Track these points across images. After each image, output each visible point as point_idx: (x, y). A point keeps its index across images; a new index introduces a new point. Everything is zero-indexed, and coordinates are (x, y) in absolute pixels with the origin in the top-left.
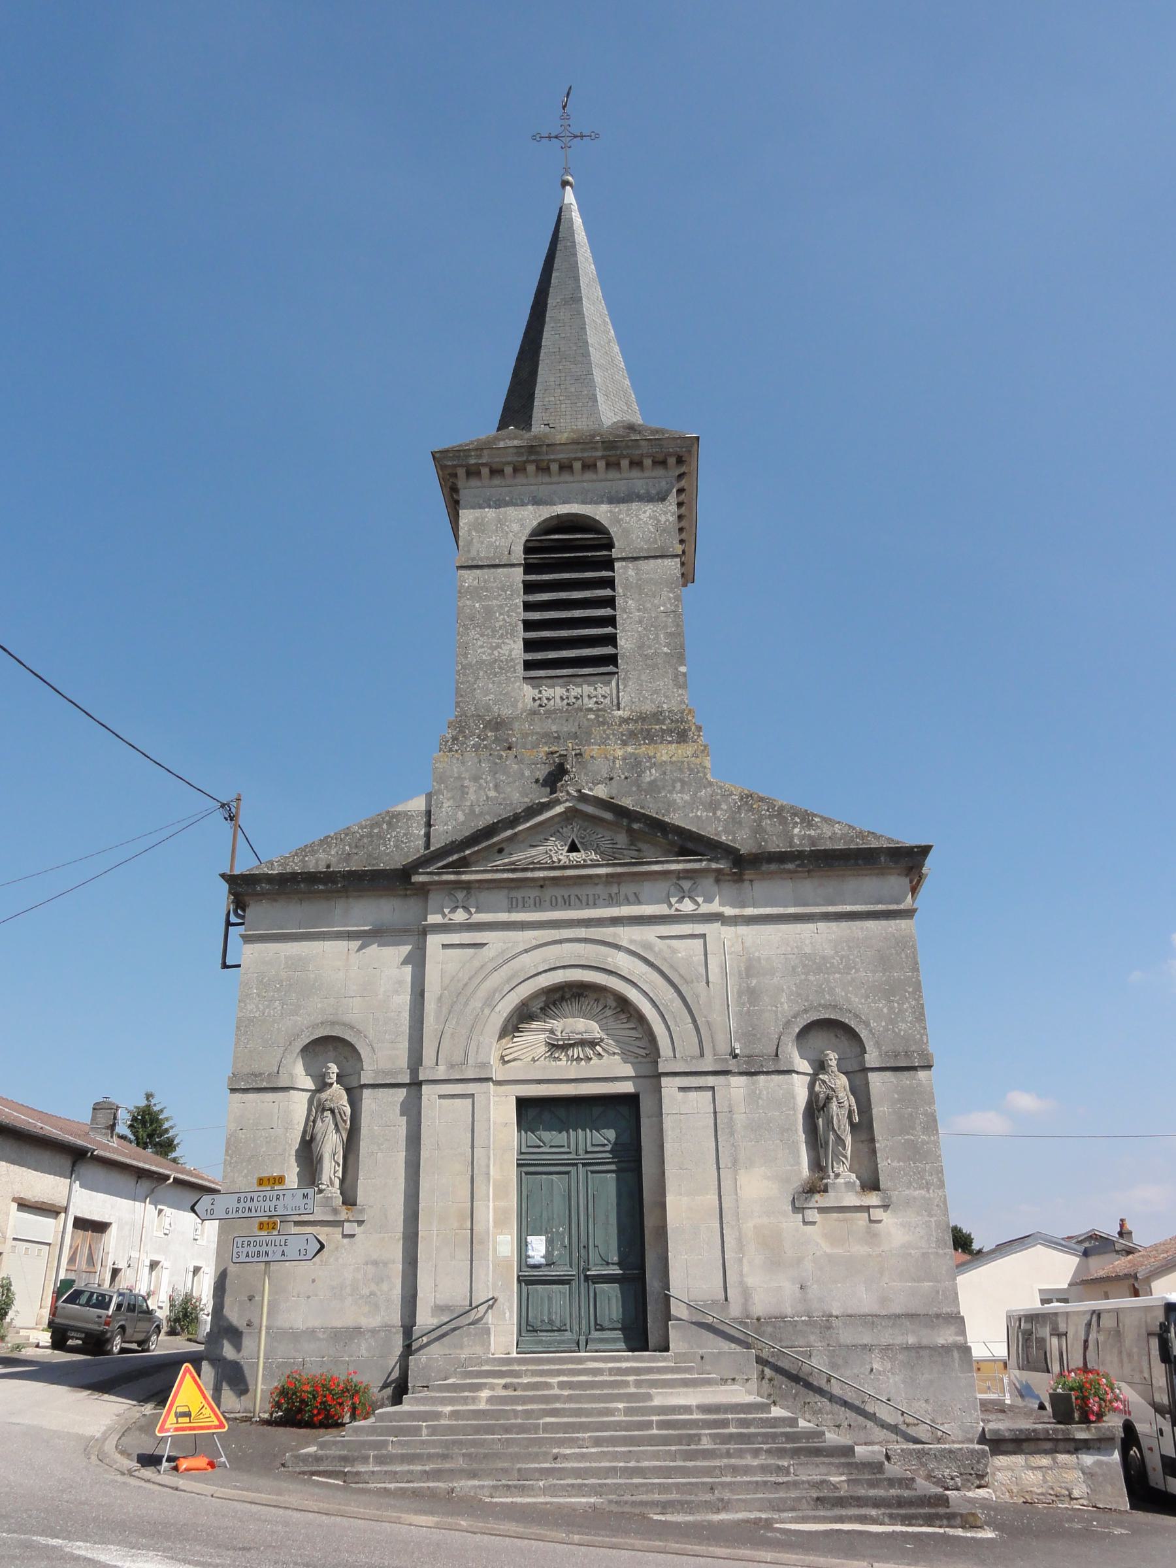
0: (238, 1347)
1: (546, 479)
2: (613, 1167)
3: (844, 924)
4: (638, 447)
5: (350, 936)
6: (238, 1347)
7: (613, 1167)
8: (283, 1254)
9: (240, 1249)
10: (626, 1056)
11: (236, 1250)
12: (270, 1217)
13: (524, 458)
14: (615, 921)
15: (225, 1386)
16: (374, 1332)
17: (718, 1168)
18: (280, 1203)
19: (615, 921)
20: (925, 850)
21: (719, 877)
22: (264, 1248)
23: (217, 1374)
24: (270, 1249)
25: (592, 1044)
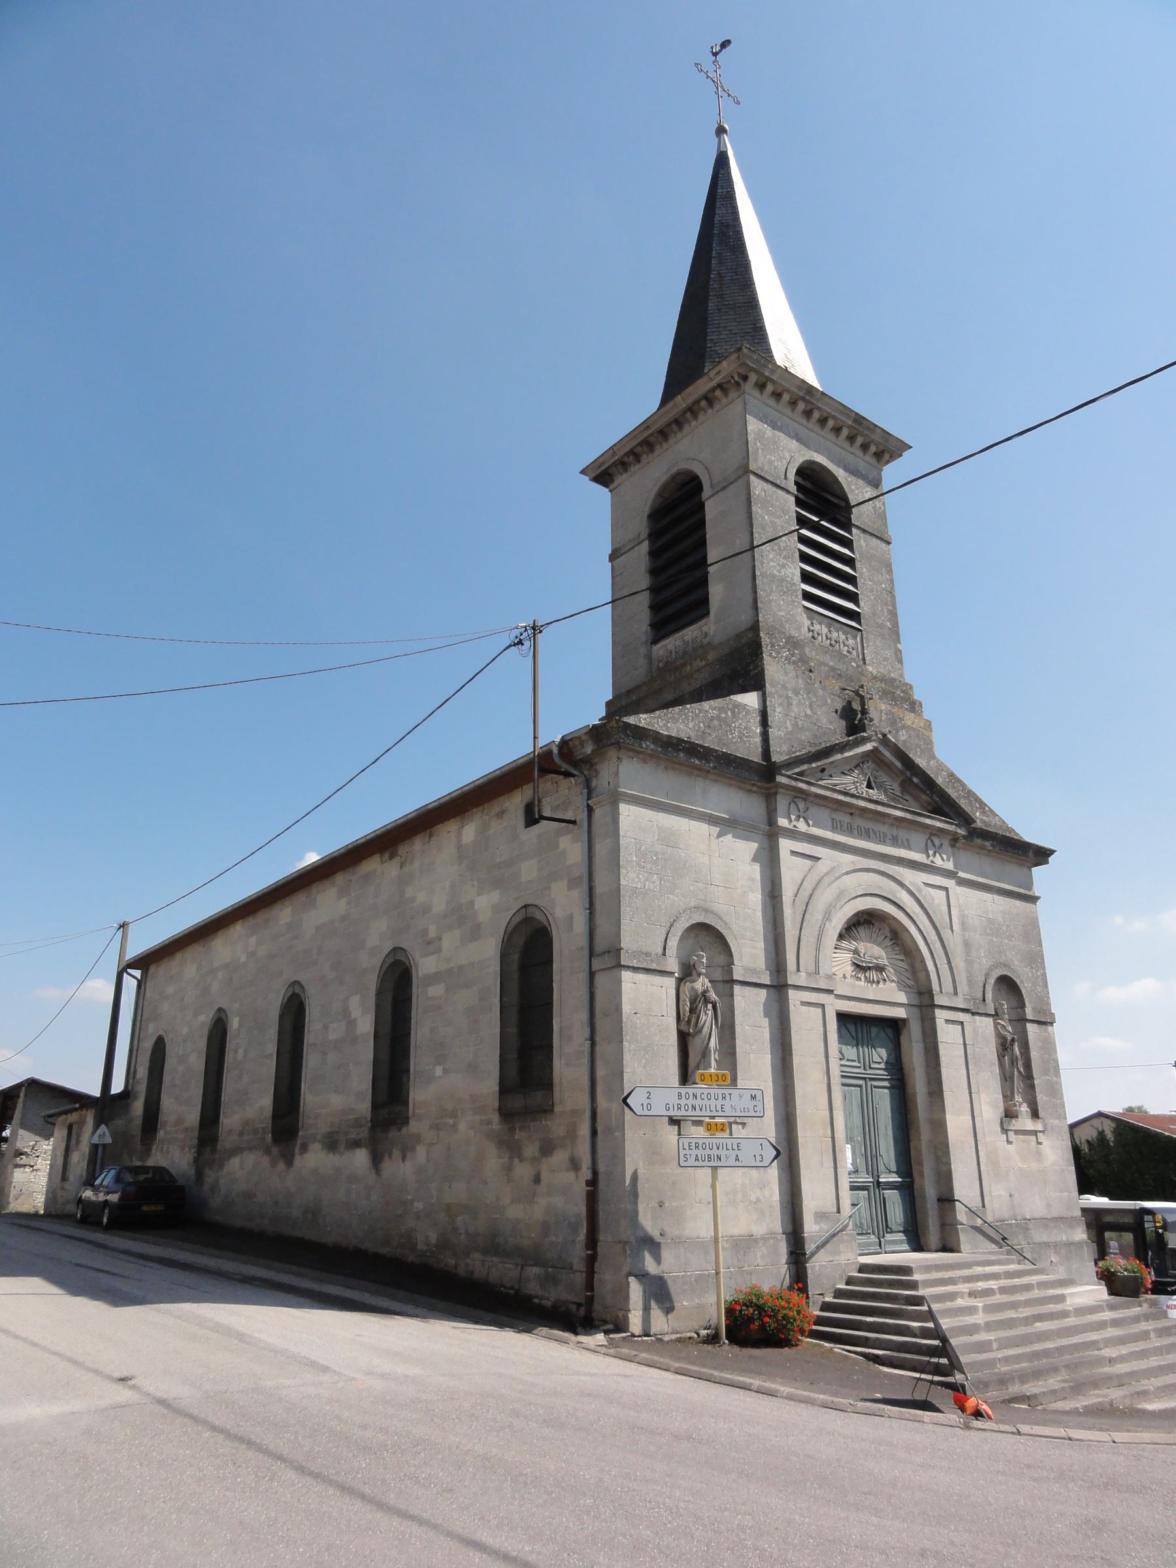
0: (658, 1259)
1: (804, 422)
2: (886, 1084)
3: (1018, 903)
4: (873, 432)
5: (712, 820)
6: (658, 1259)
7: (886, 1084)
8: (737, 1159)
9: (688, 1152)
10: (902, 986)
11: (682, 1153)
12: (713, 1117)
13: (802, 394)
14: (901, 861)
15: (653, 1304)
16: (764, 1239)
17: (970, 1093)
18: (727, 1103)
19: (901, 861)
20: (1052, 852)
21: (954, 840)
22: (715, 1152)
23: (645, 1292)
24: (723, 1153)
25: (880, 969)
